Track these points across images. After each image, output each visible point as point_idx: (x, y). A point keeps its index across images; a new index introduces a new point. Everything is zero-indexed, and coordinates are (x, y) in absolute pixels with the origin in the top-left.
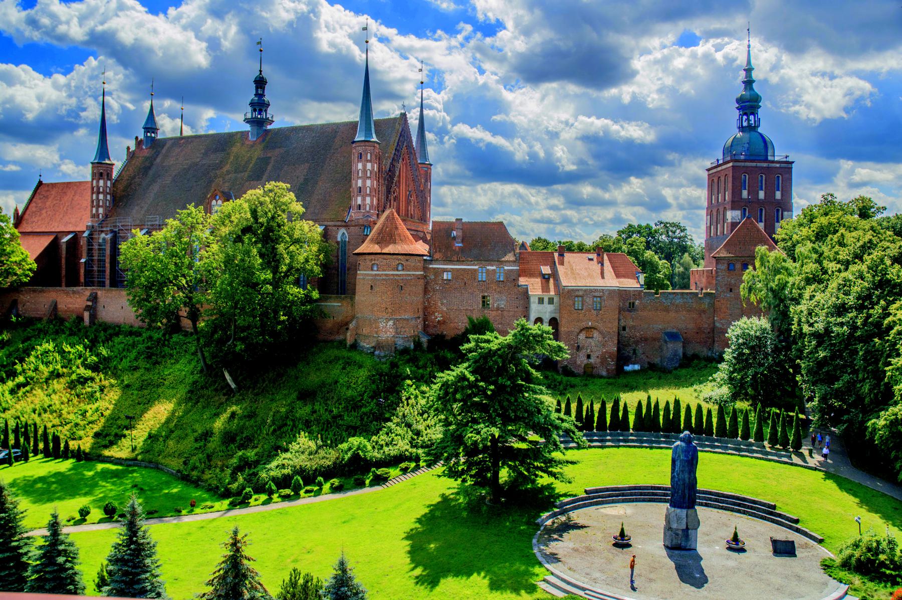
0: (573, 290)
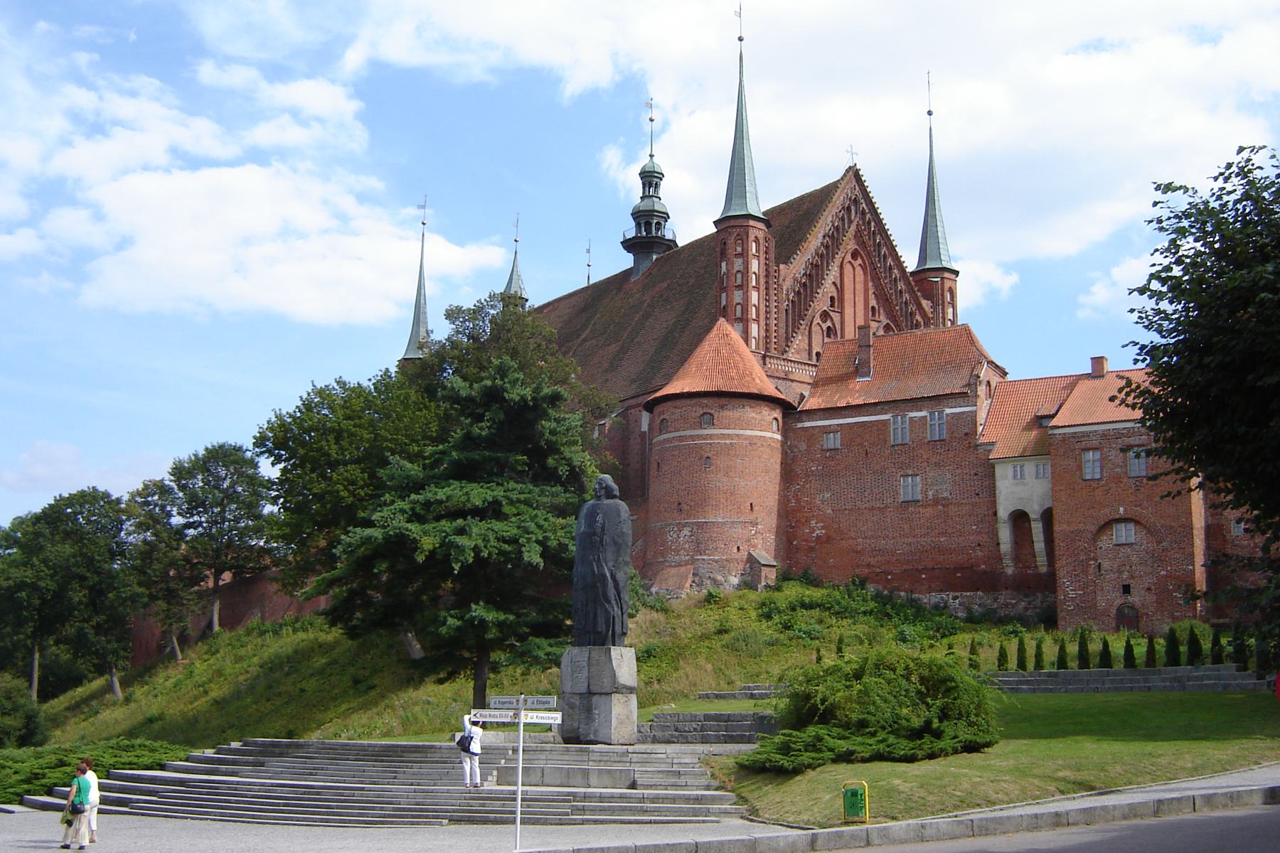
0: (1074, 435)
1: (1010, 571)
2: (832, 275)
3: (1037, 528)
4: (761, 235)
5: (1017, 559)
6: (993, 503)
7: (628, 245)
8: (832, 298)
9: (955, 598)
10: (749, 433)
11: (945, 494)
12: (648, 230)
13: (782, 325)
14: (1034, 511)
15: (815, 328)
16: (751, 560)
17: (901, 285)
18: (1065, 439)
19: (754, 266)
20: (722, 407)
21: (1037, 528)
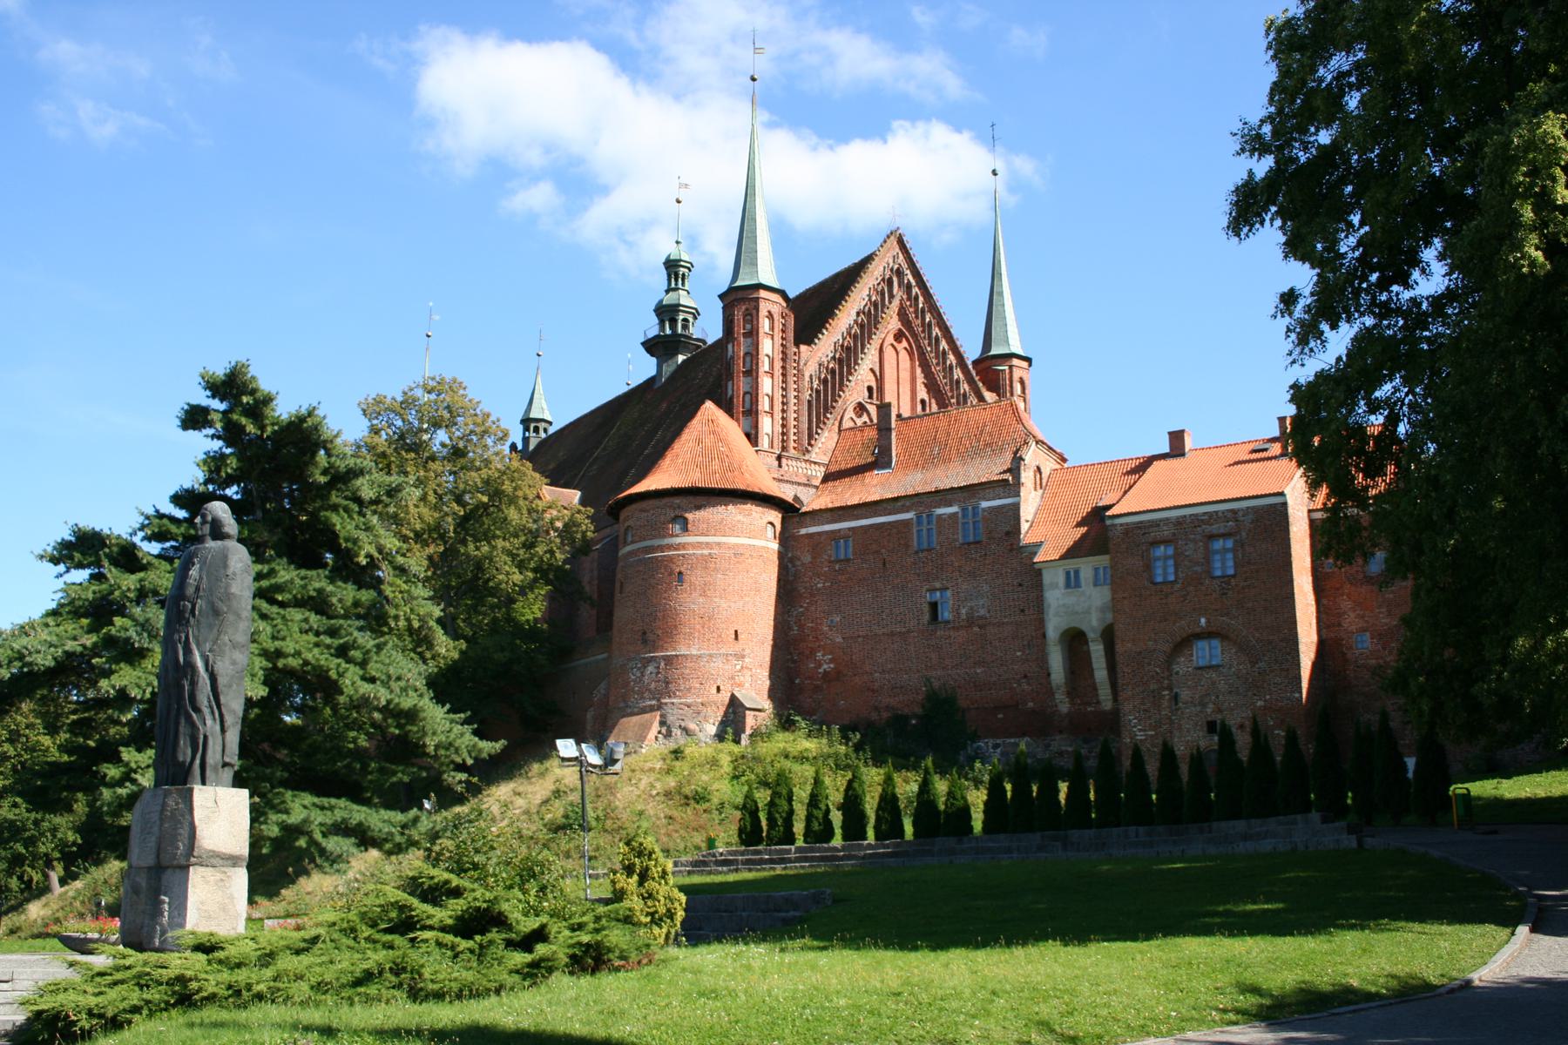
1: (1064, 708)
2: (869, 360)
3: (1097, 650)
4: (776, 310)
5: (1072, 692)
6: (1041, 623)
7: (651, 346)
8: (870, 389)
9: (996, 746)
10: (733, 540)
11: (982, 612)
12: (673, 327)
13: (805, 419)
14: (1093, 624)
16: (734, 703)
17: (958, 374)
18: (1130, 530)
19: (767, 347)
20: (698, 508)
21: (1097, 650)
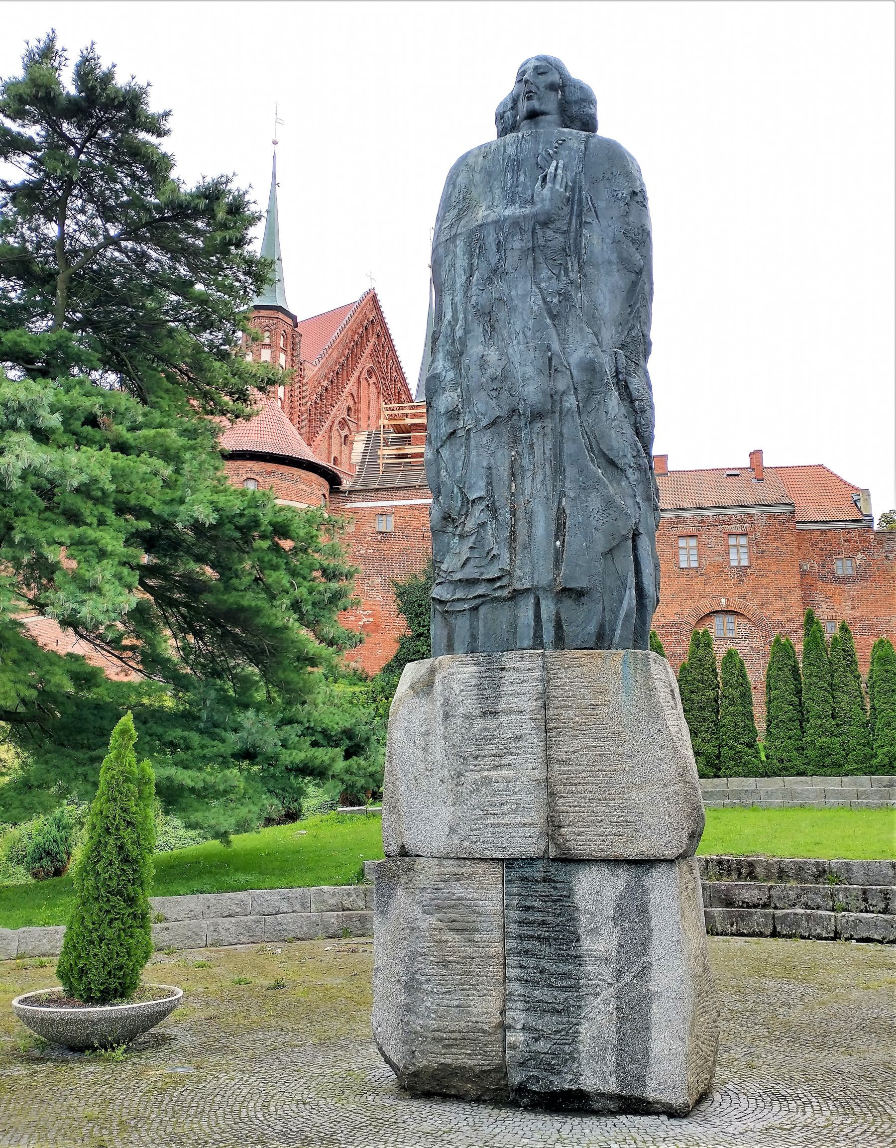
8: (349, 409)
15: (335, 434)
